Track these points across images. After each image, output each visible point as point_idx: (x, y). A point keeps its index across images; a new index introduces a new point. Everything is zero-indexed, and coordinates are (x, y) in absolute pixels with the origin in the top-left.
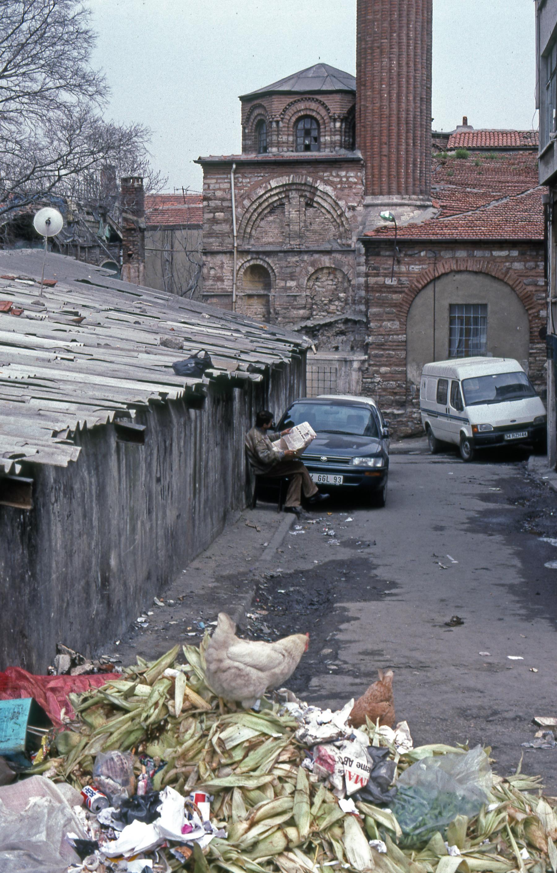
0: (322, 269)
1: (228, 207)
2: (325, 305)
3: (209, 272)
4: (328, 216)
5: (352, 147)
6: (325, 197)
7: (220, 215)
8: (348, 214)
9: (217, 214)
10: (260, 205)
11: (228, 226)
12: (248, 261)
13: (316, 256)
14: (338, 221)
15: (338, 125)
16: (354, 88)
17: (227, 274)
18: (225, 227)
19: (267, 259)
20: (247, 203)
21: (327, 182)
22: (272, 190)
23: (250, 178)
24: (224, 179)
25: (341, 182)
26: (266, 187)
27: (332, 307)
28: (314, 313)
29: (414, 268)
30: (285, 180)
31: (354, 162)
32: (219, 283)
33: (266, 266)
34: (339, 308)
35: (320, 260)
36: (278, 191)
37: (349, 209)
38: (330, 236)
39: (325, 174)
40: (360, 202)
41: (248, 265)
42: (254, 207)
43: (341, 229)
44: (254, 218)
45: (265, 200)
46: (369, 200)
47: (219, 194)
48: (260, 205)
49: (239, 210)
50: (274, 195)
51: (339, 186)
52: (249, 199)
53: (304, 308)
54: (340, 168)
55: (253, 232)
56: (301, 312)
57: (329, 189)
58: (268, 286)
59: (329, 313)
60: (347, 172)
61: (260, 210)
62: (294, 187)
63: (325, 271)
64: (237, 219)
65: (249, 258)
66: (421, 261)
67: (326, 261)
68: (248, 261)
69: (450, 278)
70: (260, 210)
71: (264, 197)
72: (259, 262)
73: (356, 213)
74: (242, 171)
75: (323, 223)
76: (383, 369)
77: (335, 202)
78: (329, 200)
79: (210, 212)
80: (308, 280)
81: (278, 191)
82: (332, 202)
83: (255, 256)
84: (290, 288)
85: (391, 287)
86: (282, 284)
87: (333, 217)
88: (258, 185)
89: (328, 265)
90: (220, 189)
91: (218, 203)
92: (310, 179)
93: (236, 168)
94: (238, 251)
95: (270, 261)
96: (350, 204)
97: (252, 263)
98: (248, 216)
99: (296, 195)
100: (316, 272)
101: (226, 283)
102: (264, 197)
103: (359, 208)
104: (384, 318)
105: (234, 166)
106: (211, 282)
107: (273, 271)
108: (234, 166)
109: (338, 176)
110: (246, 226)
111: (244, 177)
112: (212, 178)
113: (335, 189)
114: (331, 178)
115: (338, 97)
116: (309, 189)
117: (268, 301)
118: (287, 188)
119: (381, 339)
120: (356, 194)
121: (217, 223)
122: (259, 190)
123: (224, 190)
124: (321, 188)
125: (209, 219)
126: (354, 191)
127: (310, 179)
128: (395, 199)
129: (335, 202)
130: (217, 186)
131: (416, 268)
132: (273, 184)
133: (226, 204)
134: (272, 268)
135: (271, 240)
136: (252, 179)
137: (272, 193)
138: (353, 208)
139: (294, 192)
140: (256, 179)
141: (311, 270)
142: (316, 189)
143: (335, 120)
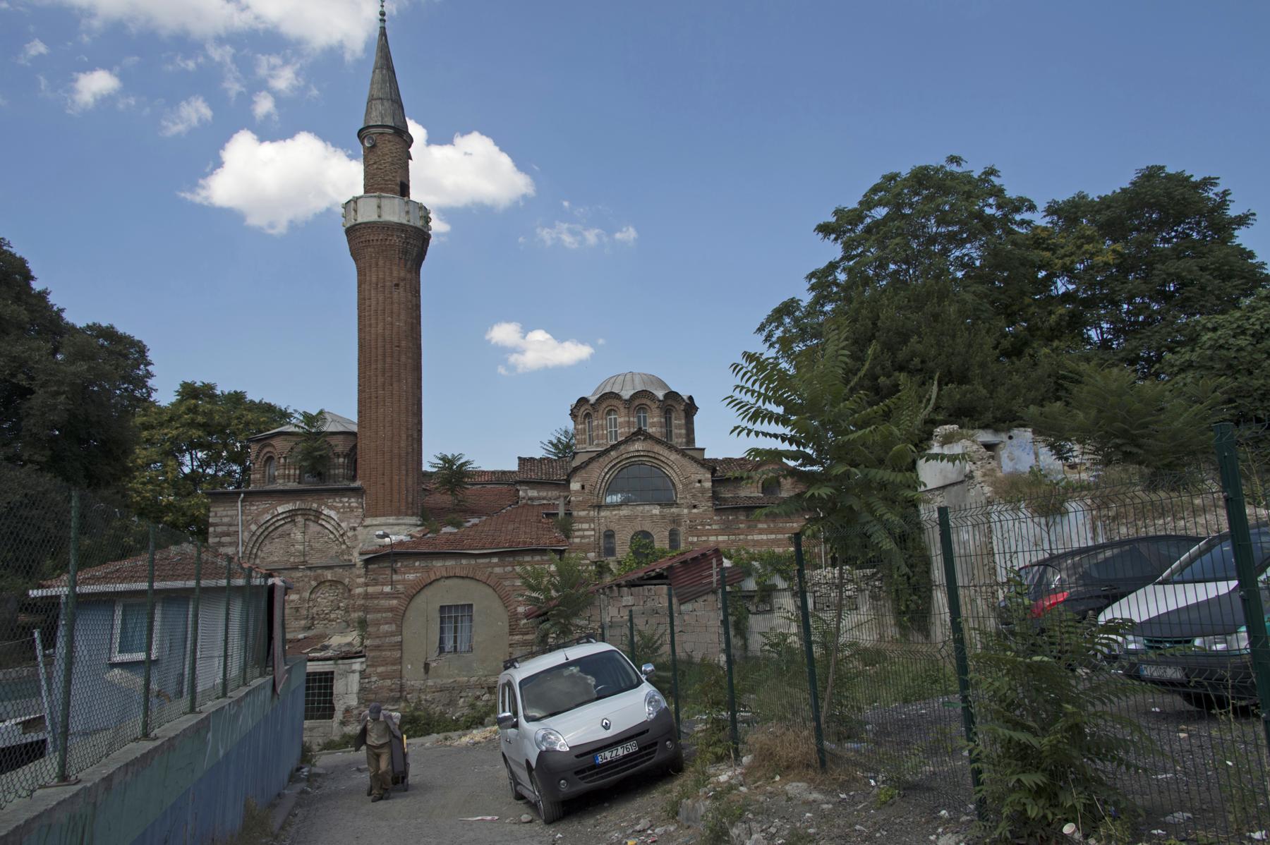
5: (354, 478)
7: (225, 539)
8: (350, 534)
13: (319, 571)
15: (341, 460)
16: (355, 429)
20: (253, 527)
21: (331, 508)
25: (343, 507)
29: (410, 575)
30: (289, 507)
31: (358, 492)
38: (333, 552)
43: (344, 547)
46: (368, 521)
47: (226, 520)
56: (303, 622)
57: (333, 514)
66: (416, 570)
67: (329, 575)
69: (442, 583)
76: (380, 669)
85: (387, 594)
88: (266, 511)
91: (225, 528)
92: (315, 505)
111: (252, 505)
115: (341, 437)
118: (292, 515)
119: (377, 642)
120: (357, 517)
123: (231, 516)
127: (315, 505)
128: (391, 520)
131: (411, 577)
132: (280, 510)
138: (354, 529)
141: (314, 583)
143: (339, 456)
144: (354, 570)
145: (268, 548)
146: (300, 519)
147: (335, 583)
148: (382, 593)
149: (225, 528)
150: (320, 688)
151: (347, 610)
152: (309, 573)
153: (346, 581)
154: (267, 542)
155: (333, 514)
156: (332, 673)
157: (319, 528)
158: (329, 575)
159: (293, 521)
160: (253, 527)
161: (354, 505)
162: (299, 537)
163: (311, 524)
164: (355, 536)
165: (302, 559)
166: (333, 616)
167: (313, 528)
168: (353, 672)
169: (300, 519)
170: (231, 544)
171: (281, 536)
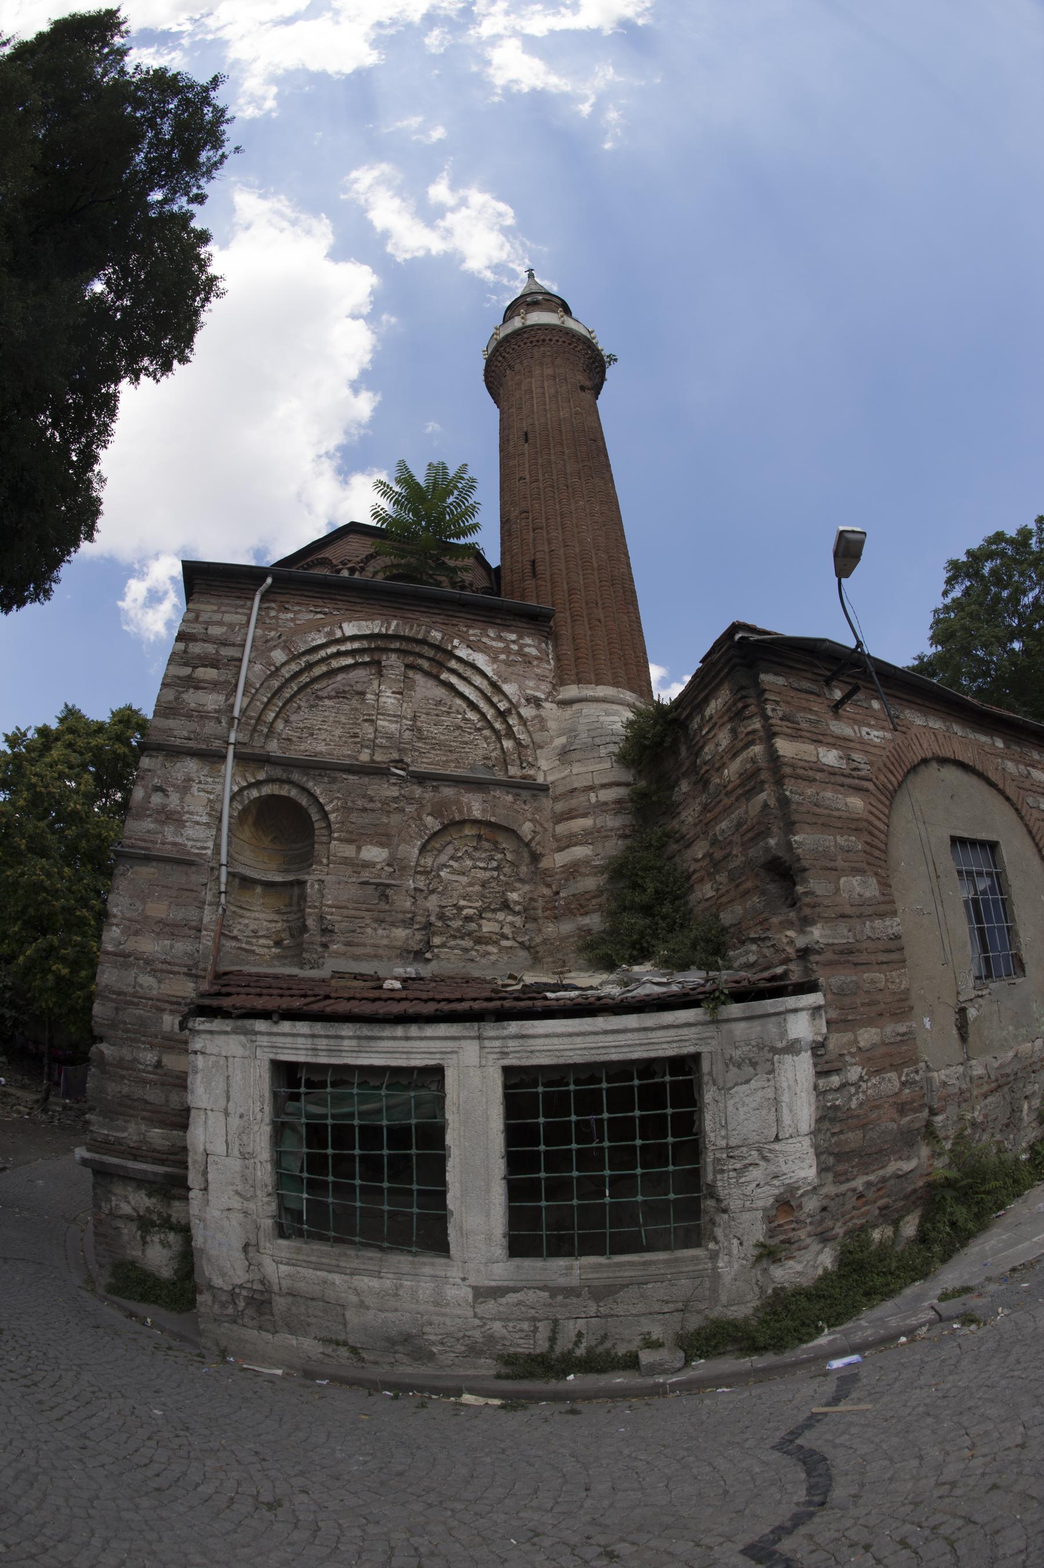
0: (463, 822)
1: (233, 659)
2: (468, 919)
3: (147, 798)
4: (472, 716)
6: (468, 673)
9: (200, 669)
10: (310, 666)
11: (222, 698)
12: (258, 784)
13: (448, 792)
14: (498, 726)
17: (197, 805)
18: (212, 701)
19: (310, 785)
20: (279, 656)
22: (345, 639)
23: (296, 613)
24: (237, 606)
26: (331, 633)
27: (488, 927)
28: (437, 940)
30: (375, 627)
32: (169, 831)
33: (304, 801)
34: (507, 930)
35: (458, 802)
36: (356, 645)
37: (528, 700)
39: (471, 632)
40: (550, 694)
41: (255, 793)
42: (294, 667)
44: (287, 693)
45: (323, 660)
46: (571, 691)
47: (215, 631)
48: (310, 666)
49: (258, 667)
50: (346, 654)
51: (503, 657)
52: (286, 648)
53: (408, 923)
54: (507, 627)
55: (280, 725)
56: (400, 933)
58: (305, 859)
59: (479, 941)
60: (521, 637)
61: (304, 679)
62: (396, 645)
63: (468, 831)
64: (248, 684)
65: (261, 776)
67: (475, 806)
68: (258, 784)
70: (304, 679)
71: (322, 653)
72: (284, 791)
73: (543, 712)
74: (280, 598)
75: (459, 728)
77: (493, 685)
78: (478, 680)
79: (186, 665)
80: (423, 850)
81: (356, 645)
82: (483, 684)
83: (278, 772)
84: (368, 865)
85: (832, 772)
86: (348, 851)
87: (483, 716)
89: (477, 814)
90: (220, 623)
91: (210, 648)
92: (436, 635)
93: (271, 586)
94: (236, 756)
95: (318, 792)
96: (529, 692)
97: (266, 790)
98: (276, 684)
99: (399, 663)
100: (445, 828)
101: (189, 832)
102: (322, 653)
103: (547, 705)
104: (839, 863)
105: (269, 580)
106: (148, 824)
107: (325, 815)
108: (269, 580)
109: (500, 638)
110: (266, 705)
112: (209, 603)
113: (495, 660)
114: (484, 640)
116: (431, 653)
117: (303, 897)
118: (375, 648)
120: (540, 678)
121: (197, 688)
122: (313, 635)
123: (231, 626)
124: (462, 652)
125: (179, 678)
126: (538, 671)
129: (493, 685)
130: (217, 617)
132: (350, 629)
133: (227, 652)
134: (321, 807)
135: (322, 748)
136: (299, 616)
137: (343, 648)
138: (536, 702)
139: (393, 656)
140: (311, 616)
141: (432, 823)
142: (452, 655)
144: (547, 803)
145: (302, 716)
146: (393, 661)
147: (493, 831)
148: (820, 768)
149: (210, 648)
150: (621, 1129)
151: (528, 912)
152: (418, 791)
153: (526, 829)
154: (302, 701)
155: (480, 660)
156: (696, 1057)
157: (440, 692)
158: (475, 806)
159: (377, 664)
160: (279, 656)
161: (534, 651)
162: (389, 700)
163: (419, 678)
164: (542, 720)
165: (395, 756)
166: (488, 927)
167: (425, 689)
168: (793, 1048)
169: (393, 661)
170: (215, 686)
171: (340, 695)
